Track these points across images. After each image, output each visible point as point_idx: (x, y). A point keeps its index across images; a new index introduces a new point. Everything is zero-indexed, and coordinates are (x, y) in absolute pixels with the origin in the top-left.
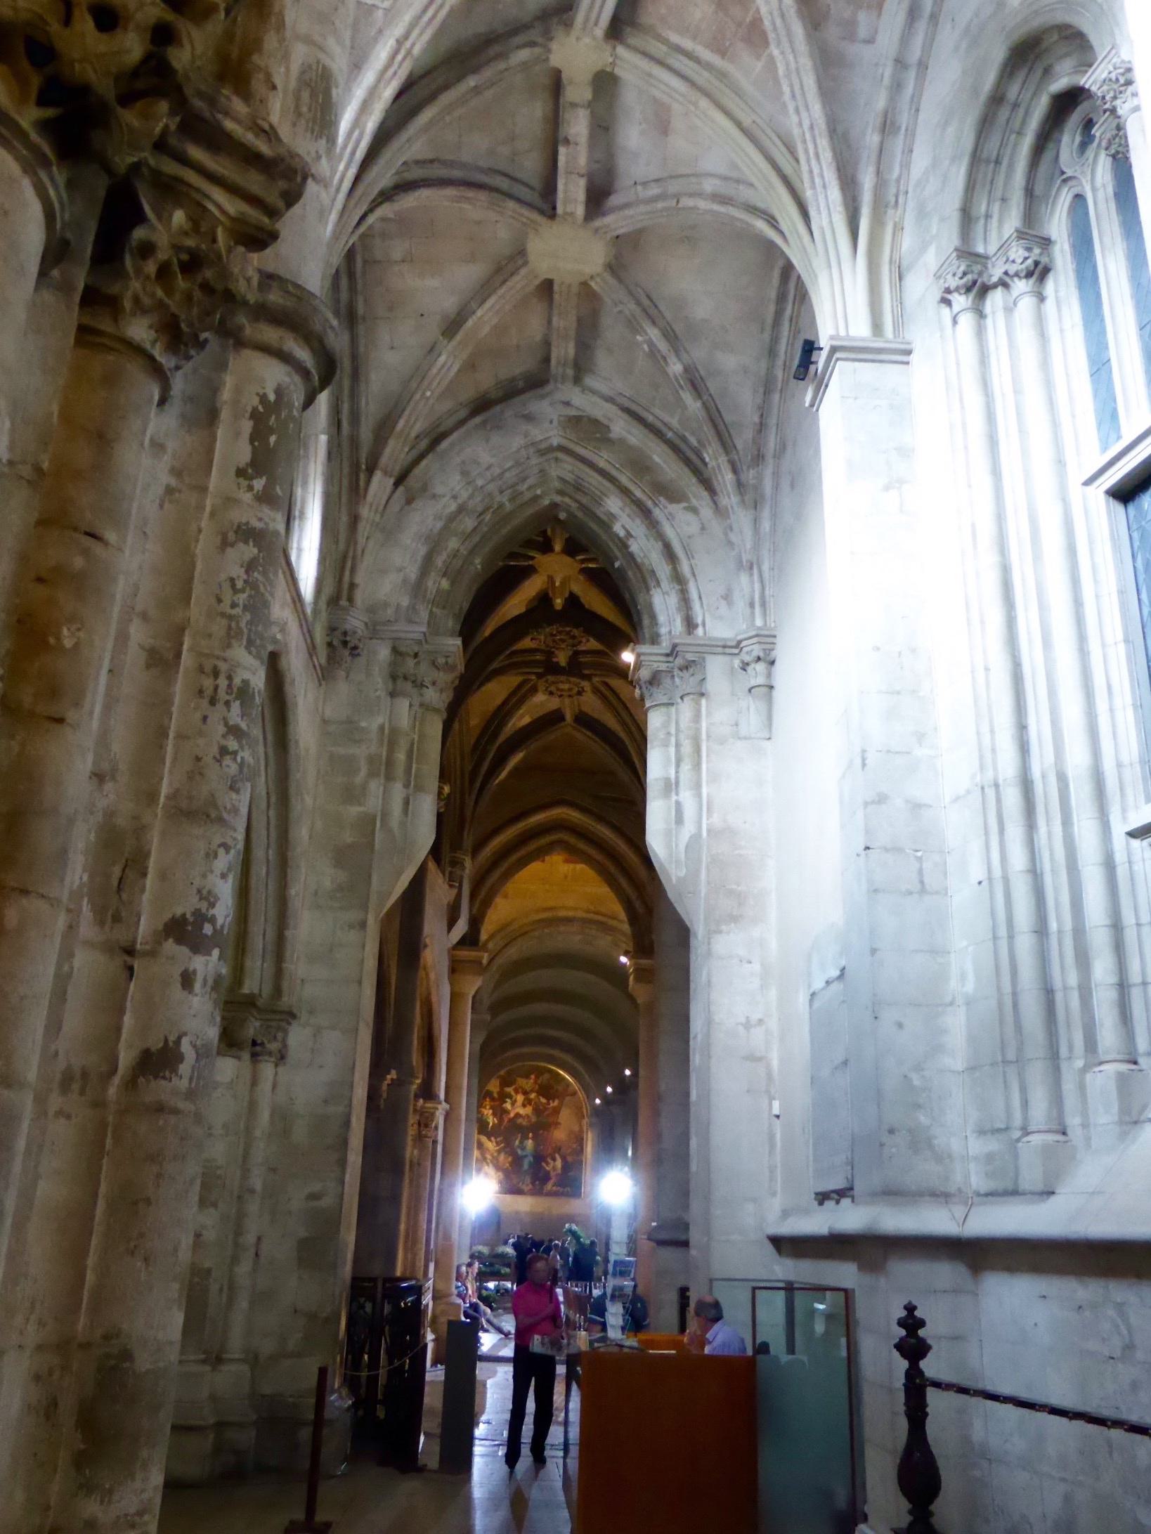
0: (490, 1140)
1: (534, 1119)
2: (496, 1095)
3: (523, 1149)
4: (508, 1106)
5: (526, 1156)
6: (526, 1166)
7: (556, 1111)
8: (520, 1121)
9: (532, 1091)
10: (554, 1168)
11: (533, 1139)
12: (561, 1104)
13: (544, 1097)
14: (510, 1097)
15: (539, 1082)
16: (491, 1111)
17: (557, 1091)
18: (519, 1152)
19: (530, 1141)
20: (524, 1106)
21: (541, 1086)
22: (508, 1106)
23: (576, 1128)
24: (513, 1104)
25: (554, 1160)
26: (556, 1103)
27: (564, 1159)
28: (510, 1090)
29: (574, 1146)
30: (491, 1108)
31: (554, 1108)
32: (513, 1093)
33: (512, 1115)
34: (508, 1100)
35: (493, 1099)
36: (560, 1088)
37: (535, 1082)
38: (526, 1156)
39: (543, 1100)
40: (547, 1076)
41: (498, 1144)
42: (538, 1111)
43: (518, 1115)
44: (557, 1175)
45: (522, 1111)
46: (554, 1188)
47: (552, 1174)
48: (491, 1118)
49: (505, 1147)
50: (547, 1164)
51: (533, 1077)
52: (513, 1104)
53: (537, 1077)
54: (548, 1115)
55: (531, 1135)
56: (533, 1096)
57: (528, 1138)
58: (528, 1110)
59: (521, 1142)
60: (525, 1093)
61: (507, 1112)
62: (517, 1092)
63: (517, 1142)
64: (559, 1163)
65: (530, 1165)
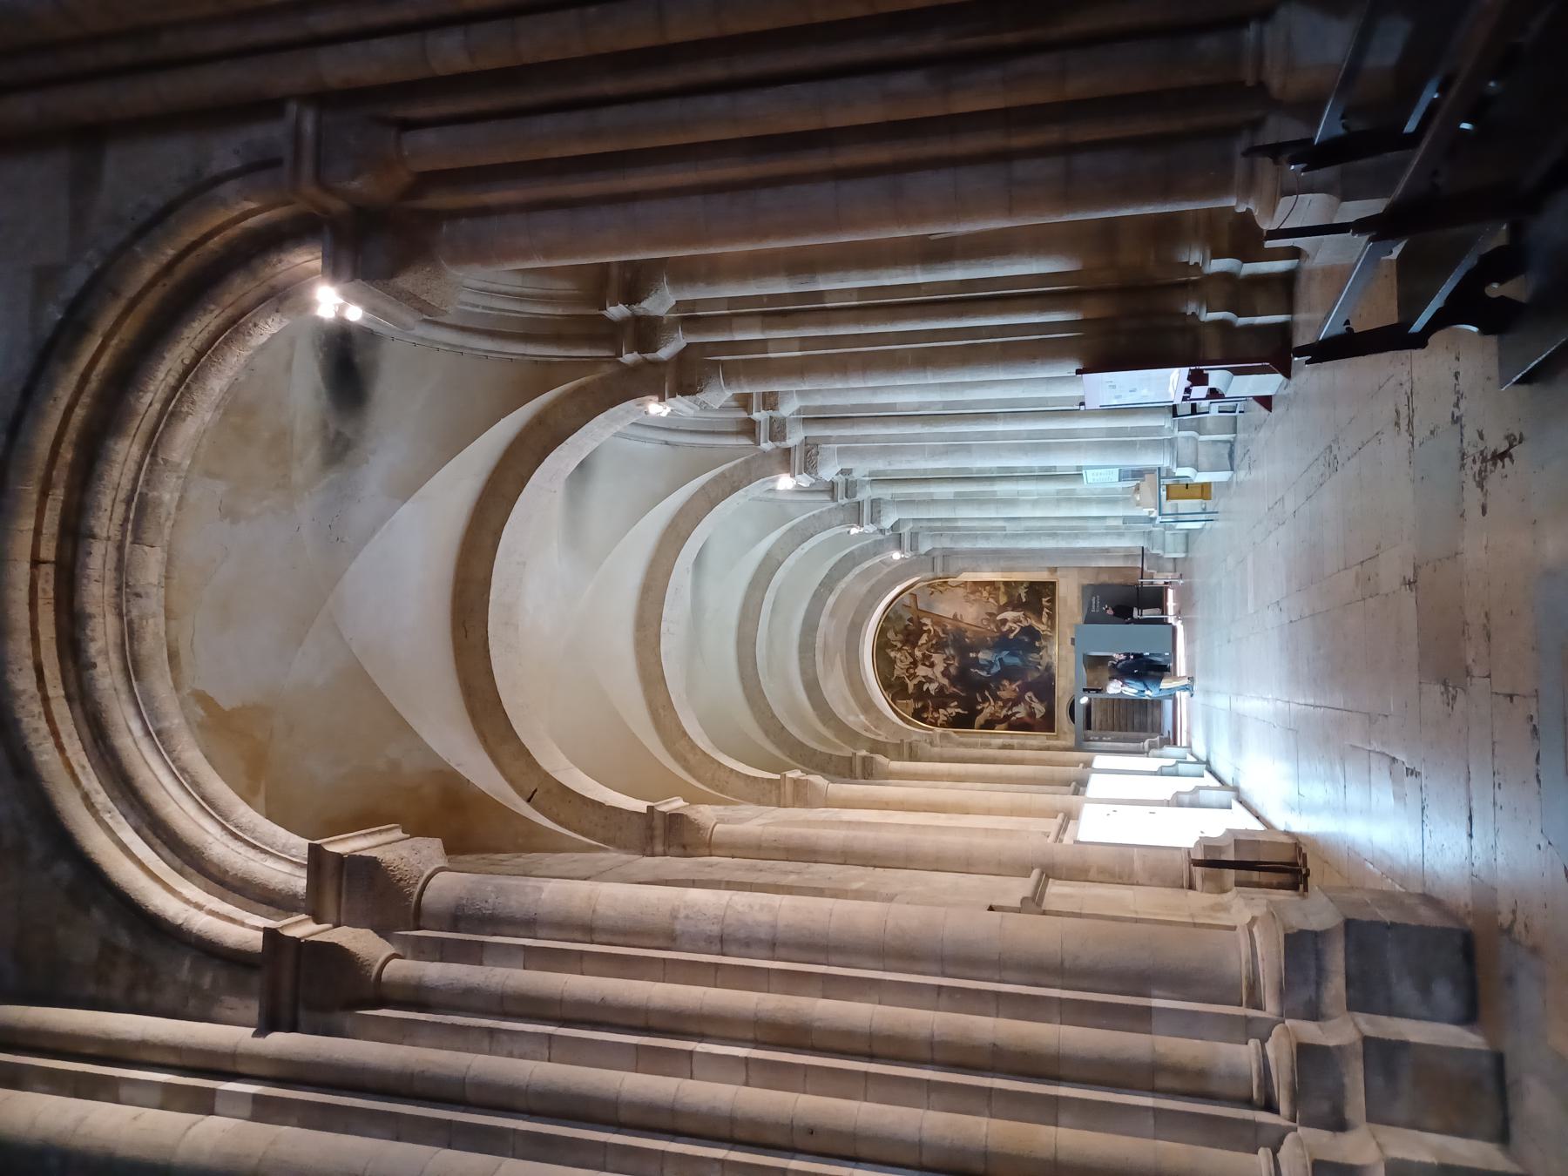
0: (982, 710)
1: (950, 651)
2: (919, 705)
3: (991, 664)
4: (933, 687)
5: (1001, 660)
6: (1016, 661)
7: (938, 620)
8: (952, 670)
9: (912, 655)
10: (1016, 621)
11: (977, 652)
12: (928, 614)
13: (919, 638)
14: (921, 684)
15: (899, 645)
16: (941, 711)
17: (910, 620)
18: (995, 670)
19: (981, 655)
20: (932, 665)
21: (905, 643)
22: (933, 687)
23: (961, 591)
24: (930, 680)
25: (1004, 621)
26: (925, 620)
27: (1003, 609)
28: (911, 685)
29: (985, 594)
30: (936, 710)
31: (934, 624)
32: (916, 681)
33: (945, 682)
34: (925, 689)
35: (925, 708)
36: (907, 616)
37: (900, 650)
38: (1001, 660)
39: (924, 638)
40: (891, 635)
41: (985, 700)
42: (939, 646)
43: (945, 673)
44: (1026, 617)
45: (940, 667)
46: (1044, 620)
47: (1025, 624)
48: (950, 710)
49: (989, 689)
50: (1011, 630)
51: (893, 654)
52: (930, 680)
53: (893, 647)
54: (944, 632)
55: (971, 655)
56: (918, 653)
57: (977, 658)
58: (937, 658)
59: (982, 668)
60: (915, 664)
61: (941, 689)
62: (914, 676)
63: (984, 674)
64: (1009, 615)
65: (1012, 654)
